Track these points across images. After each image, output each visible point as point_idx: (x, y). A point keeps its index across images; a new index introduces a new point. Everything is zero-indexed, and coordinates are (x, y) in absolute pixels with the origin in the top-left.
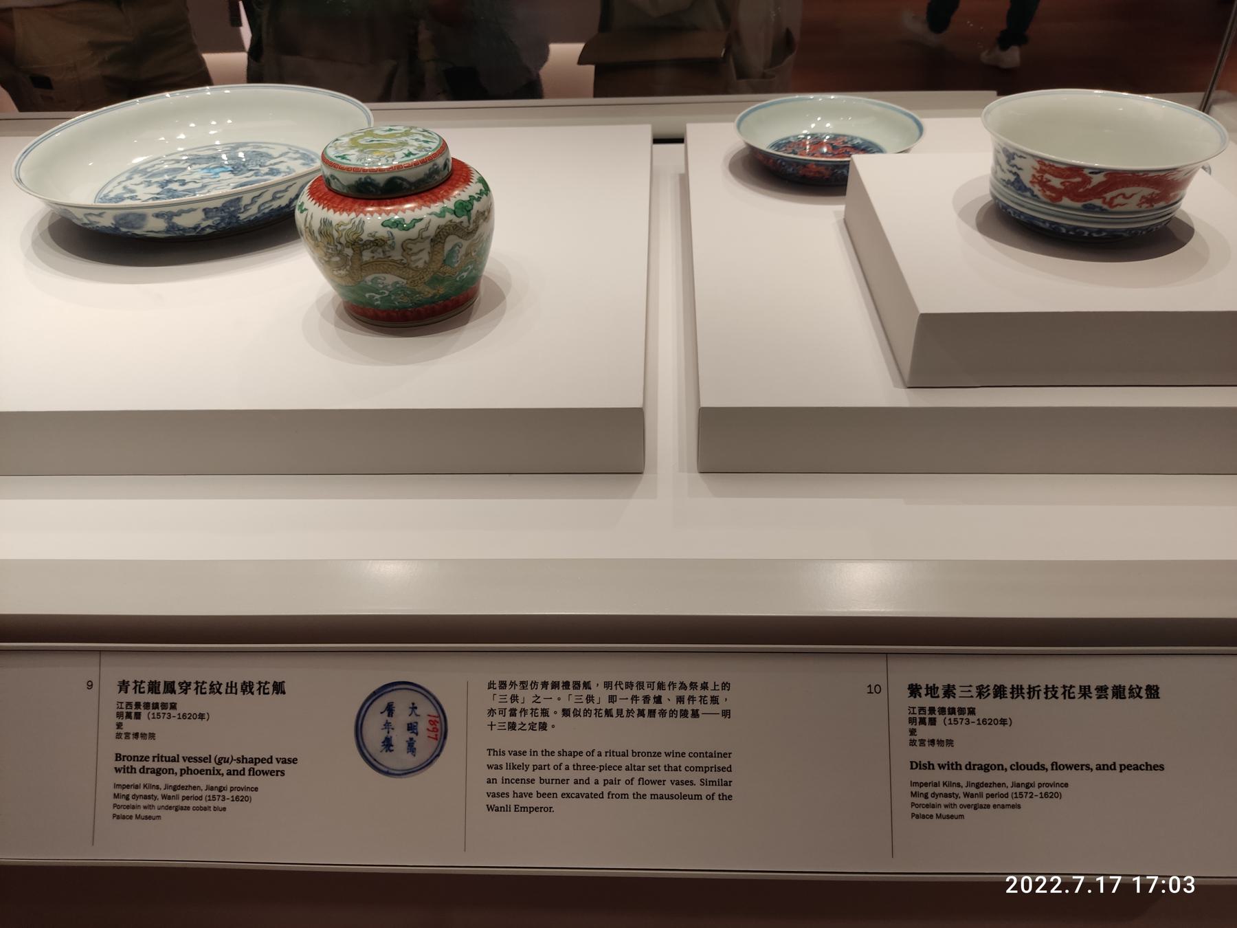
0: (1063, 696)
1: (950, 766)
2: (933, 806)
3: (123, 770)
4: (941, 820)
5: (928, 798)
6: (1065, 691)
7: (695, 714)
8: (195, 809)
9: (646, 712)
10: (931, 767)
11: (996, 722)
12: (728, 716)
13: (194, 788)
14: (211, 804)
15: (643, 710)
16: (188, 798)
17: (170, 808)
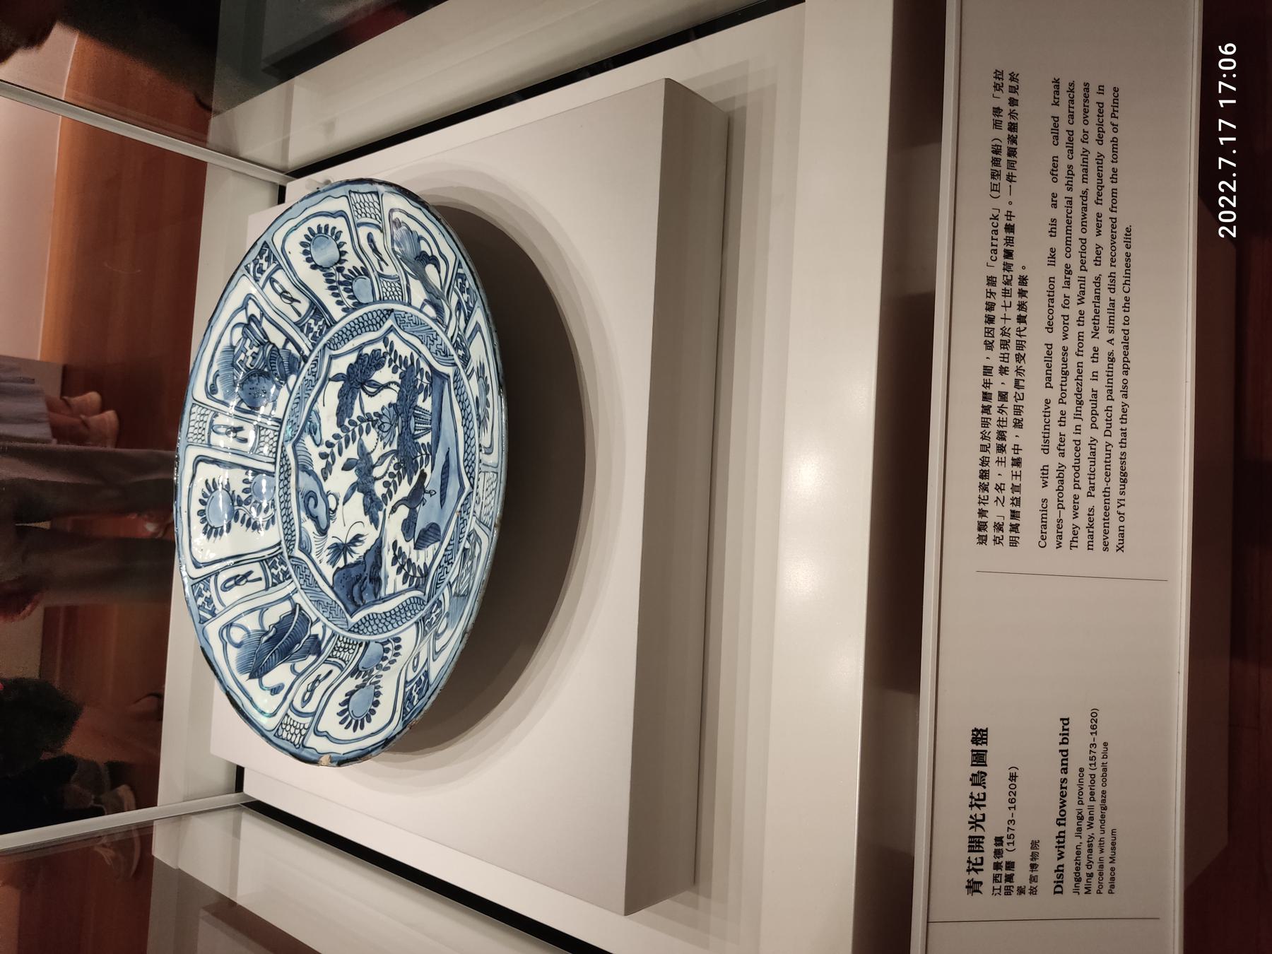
0: (981, 808)
1: (1061, 845)
2: (1101, 866)
3: (1060, 849)
4: (1117, 857)
5: (1092, 873)
6: (973, 869)
7: (1023, 280)
8: (1104, 783)
9: (1014, 522)
10: (1061, 868)
11: (1013, 787)
12: (1021, 408)
13: (1078, 853)
14: (1099, 761)
15: (1011, 525)
16: (1092, 794)
17: (1103, 816)
